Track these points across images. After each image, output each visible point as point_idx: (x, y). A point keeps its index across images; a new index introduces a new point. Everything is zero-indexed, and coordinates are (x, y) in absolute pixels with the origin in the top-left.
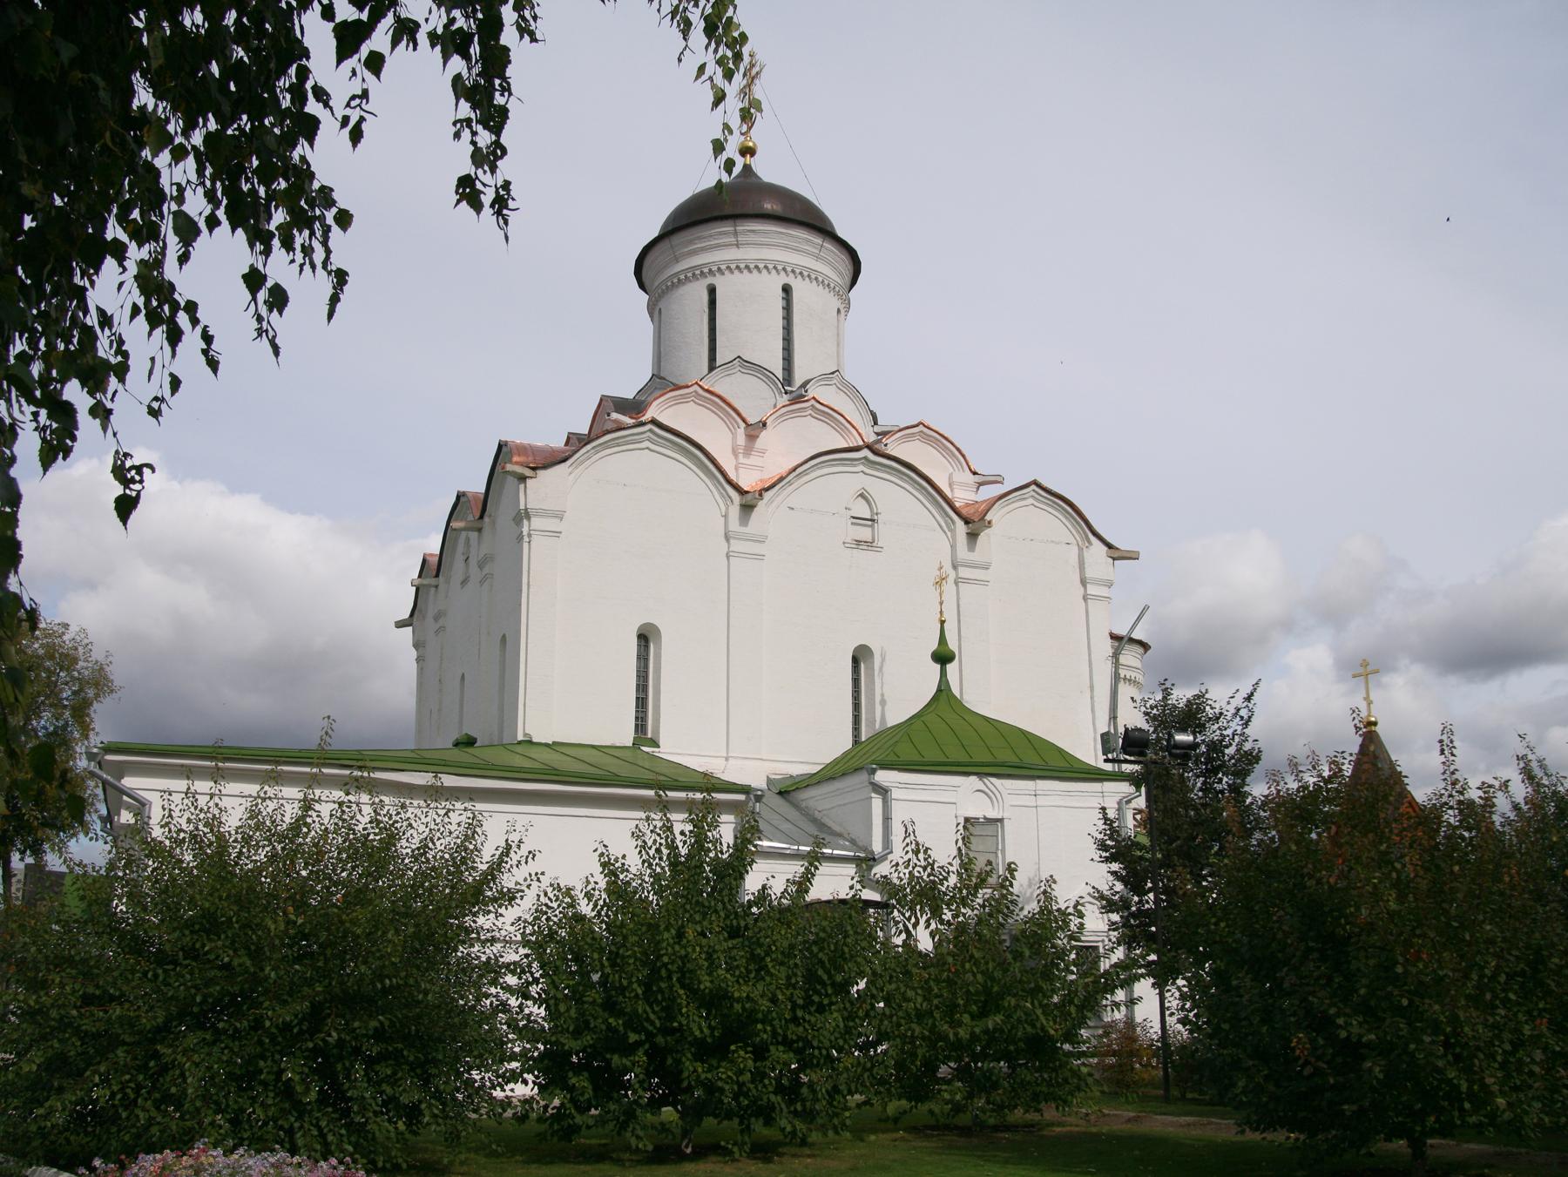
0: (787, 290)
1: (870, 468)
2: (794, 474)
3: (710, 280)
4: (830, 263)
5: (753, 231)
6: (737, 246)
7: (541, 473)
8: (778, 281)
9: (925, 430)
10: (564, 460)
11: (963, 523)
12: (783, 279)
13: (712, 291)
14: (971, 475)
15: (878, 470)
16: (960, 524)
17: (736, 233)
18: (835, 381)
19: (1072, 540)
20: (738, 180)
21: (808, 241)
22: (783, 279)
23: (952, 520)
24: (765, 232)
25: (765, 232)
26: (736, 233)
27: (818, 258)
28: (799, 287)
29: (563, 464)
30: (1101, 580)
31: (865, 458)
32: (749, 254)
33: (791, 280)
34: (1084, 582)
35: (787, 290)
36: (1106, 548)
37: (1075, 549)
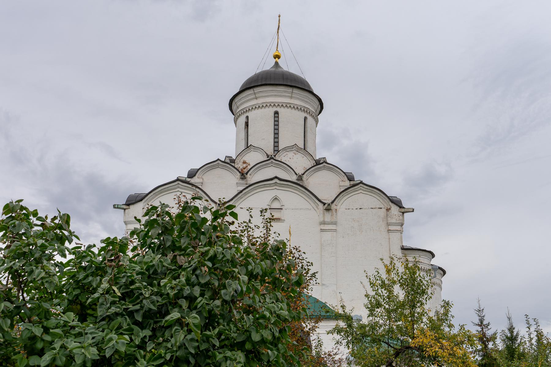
0: (276, 113)
1: (279, 186)
2: (241, 194)
4: (298, 99)
5: (261, 92)
6: (256, 98)
7: (131, 207)
8: (272, 110)
9: (326, 165)
10: (141, 200)
11: (322, 205)
12: (275, 109)
13: (247, 117)
14: (349, 181)
15: (283, 187)
16: (321, 205)
17: (255, 94)
18: (295, 149)
20: (271, 69)
21: (285, 92)
22: (275, 109)
23: (317, 203)
24: (266, 91)
25: (266, 91)
26: (255, 94)
27: (291, 97)
28: (281, 110)
29: (141, 202)
30: (396, 223)
31: (276, 182)
32: (260, 101)
33: (278, 109)
34: (388, 224)
35: (276, 113)
36: (398, 208)
37: (384, 210)
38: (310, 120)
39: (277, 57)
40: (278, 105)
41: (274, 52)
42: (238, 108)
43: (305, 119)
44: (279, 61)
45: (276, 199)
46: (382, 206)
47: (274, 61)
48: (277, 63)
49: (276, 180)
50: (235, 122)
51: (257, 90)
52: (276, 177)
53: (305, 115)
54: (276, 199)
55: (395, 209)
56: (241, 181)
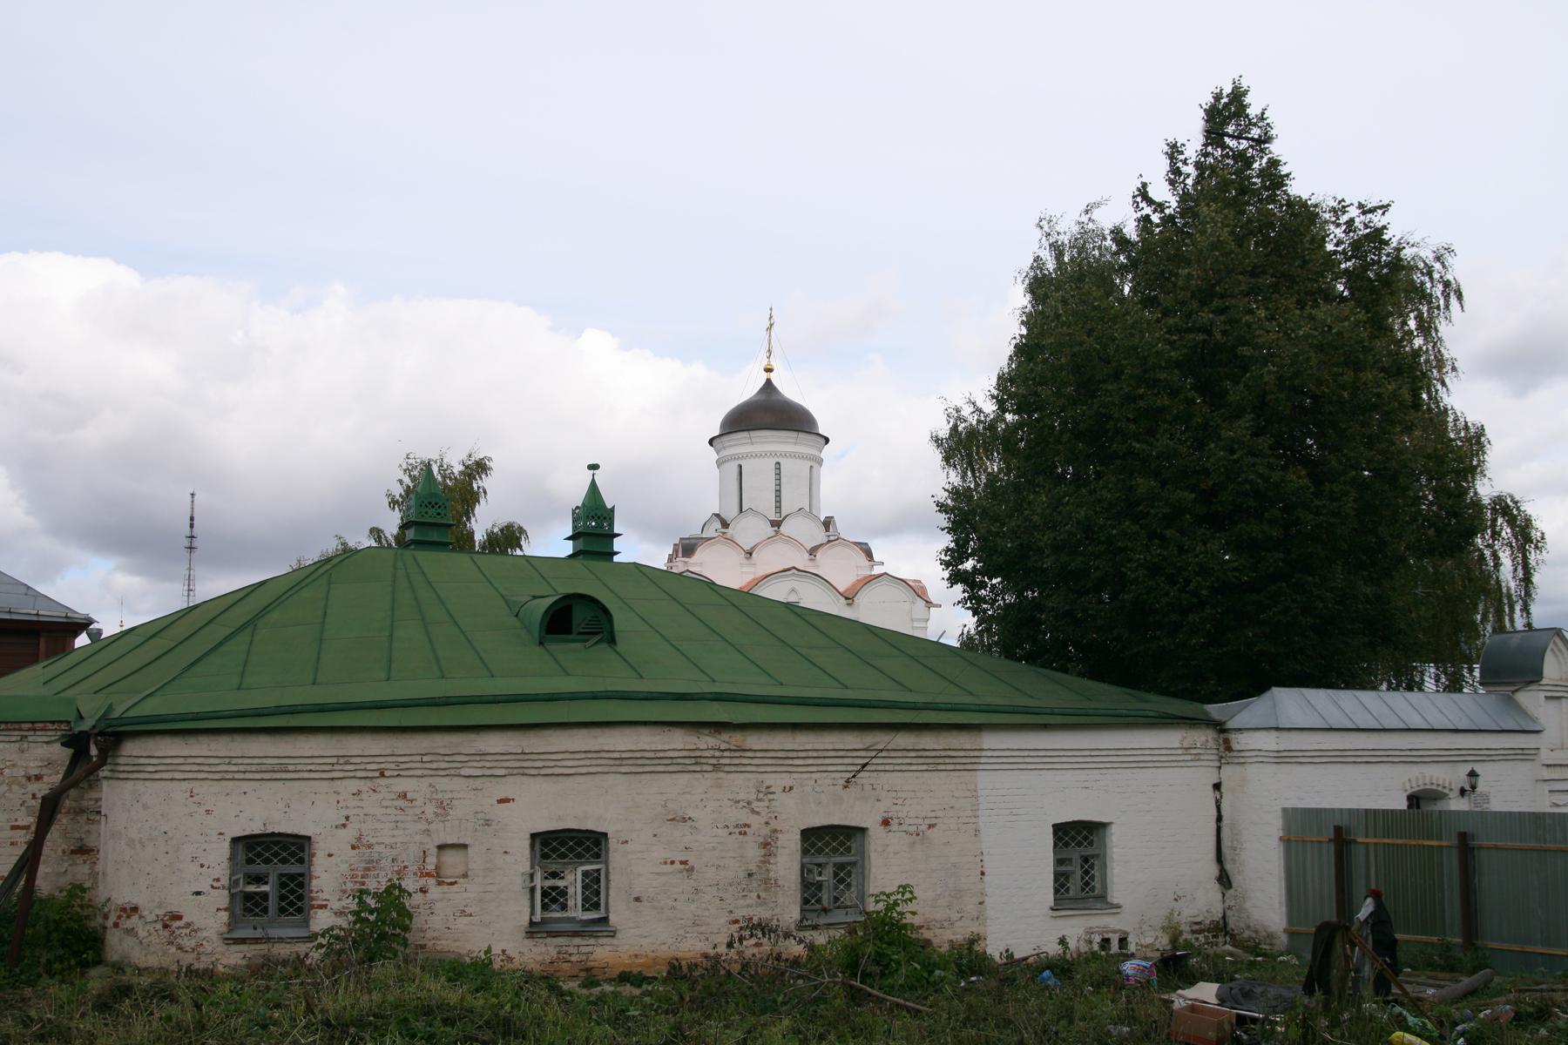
3: (739, 462)
8: (771, 462)
13: (740, 467)
19: (908, 600)
27: (796, 444)
34: (912, 620)
38: (816, 466)
39: (769, 370)
40: (781, 455)
41: (764, 363)
42: (724, 448)
43: (811, 467)
44: (773, 376)
45: (793, 590)
46: (908, 600)
47: (763, 377)
48: (769, 382)
49: (794, 571)
50: (719, 463)
51: (753, 434)
52: (794, 568)
53: (810, 463)
54: (793, 590)
55: (921, 603)
56: (747, 562)
